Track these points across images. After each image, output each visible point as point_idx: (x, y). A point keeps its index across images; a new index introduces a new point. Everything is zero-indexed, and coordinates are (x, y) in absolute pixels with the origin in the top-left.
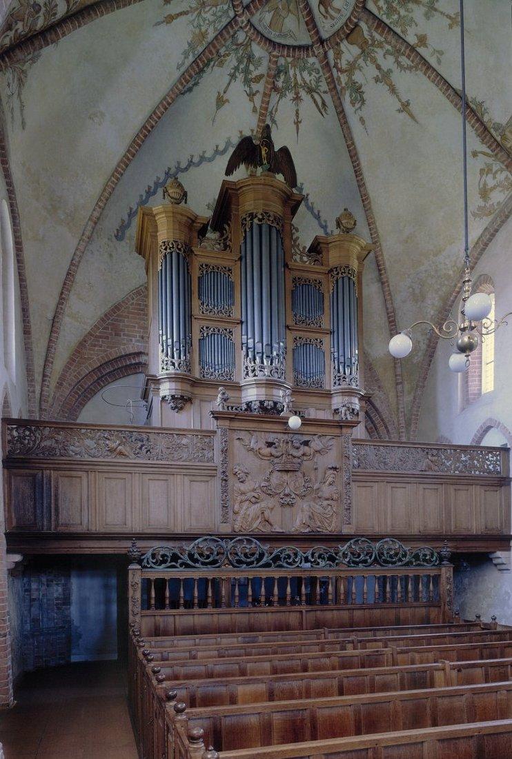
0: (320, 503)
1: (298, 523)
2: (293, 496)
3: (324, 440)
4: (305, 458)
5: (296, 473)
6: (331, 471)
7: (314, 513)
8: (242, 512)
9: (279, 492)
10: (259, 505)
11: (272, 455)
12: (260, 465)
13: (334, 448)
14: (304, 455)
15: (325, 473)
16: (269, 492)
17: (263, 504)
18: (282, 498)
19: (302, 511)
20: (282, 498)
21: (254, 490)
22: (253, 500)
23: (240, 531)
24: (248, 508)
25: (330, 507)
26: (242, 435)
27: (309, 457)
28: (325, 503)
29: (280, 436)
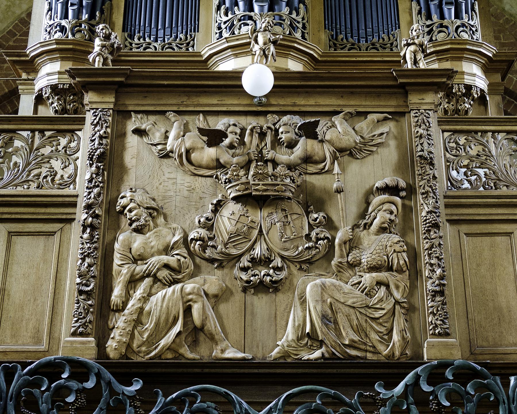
0: (355, 280)
1: (290, 334)
2: (278, 262)
3: (363, 125)
4: (312, 168)
5: (284, 205)
6: (385, 197)
7: (335, 306)
8: (132, 304)
9: (234, 252)
10: (179, 286)
11: (219, 165)
12: (191, 190)
13: (392, 143)
14: (308, 159)
15: (368, 204)
16: (209, 253)
17: (189, 287)
18: (245, 269)
19: (303, 301)
20: (245, 269)
21: (167, 250)
22: (164, 274)
23: (125, 356)
24: (150, 295)
25: (383, 289)
26: (145, 125)
27: (321, 166)
28: (368, 278)
29: (243, 121)
